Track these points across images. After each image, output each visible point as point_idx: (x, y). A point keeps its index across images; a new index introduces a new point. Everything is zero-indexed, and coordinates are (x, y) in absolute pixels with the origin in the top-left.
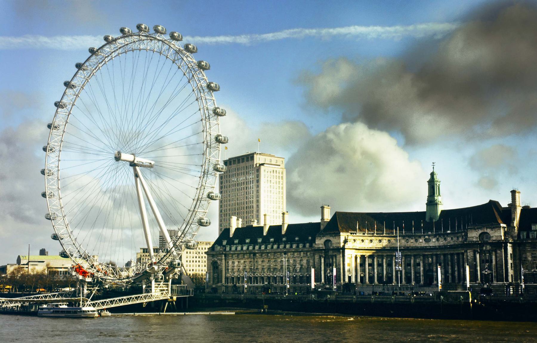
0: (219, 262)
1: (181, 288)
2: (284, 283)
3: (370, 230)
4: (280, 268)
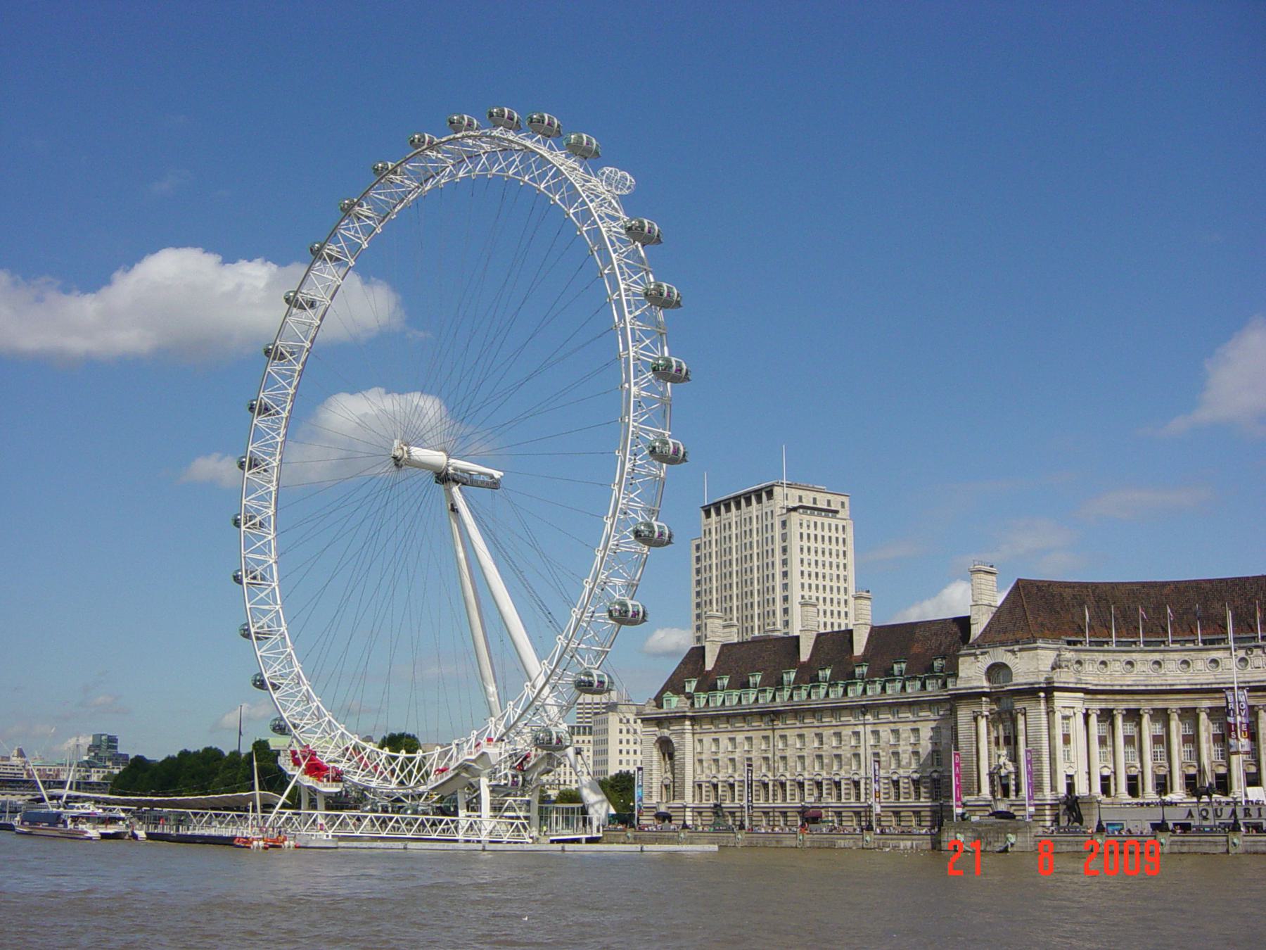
0: (674, 739)
1: (567, 813)
2: (862, 800)
3: (1125, 633)
4: (849, 755)
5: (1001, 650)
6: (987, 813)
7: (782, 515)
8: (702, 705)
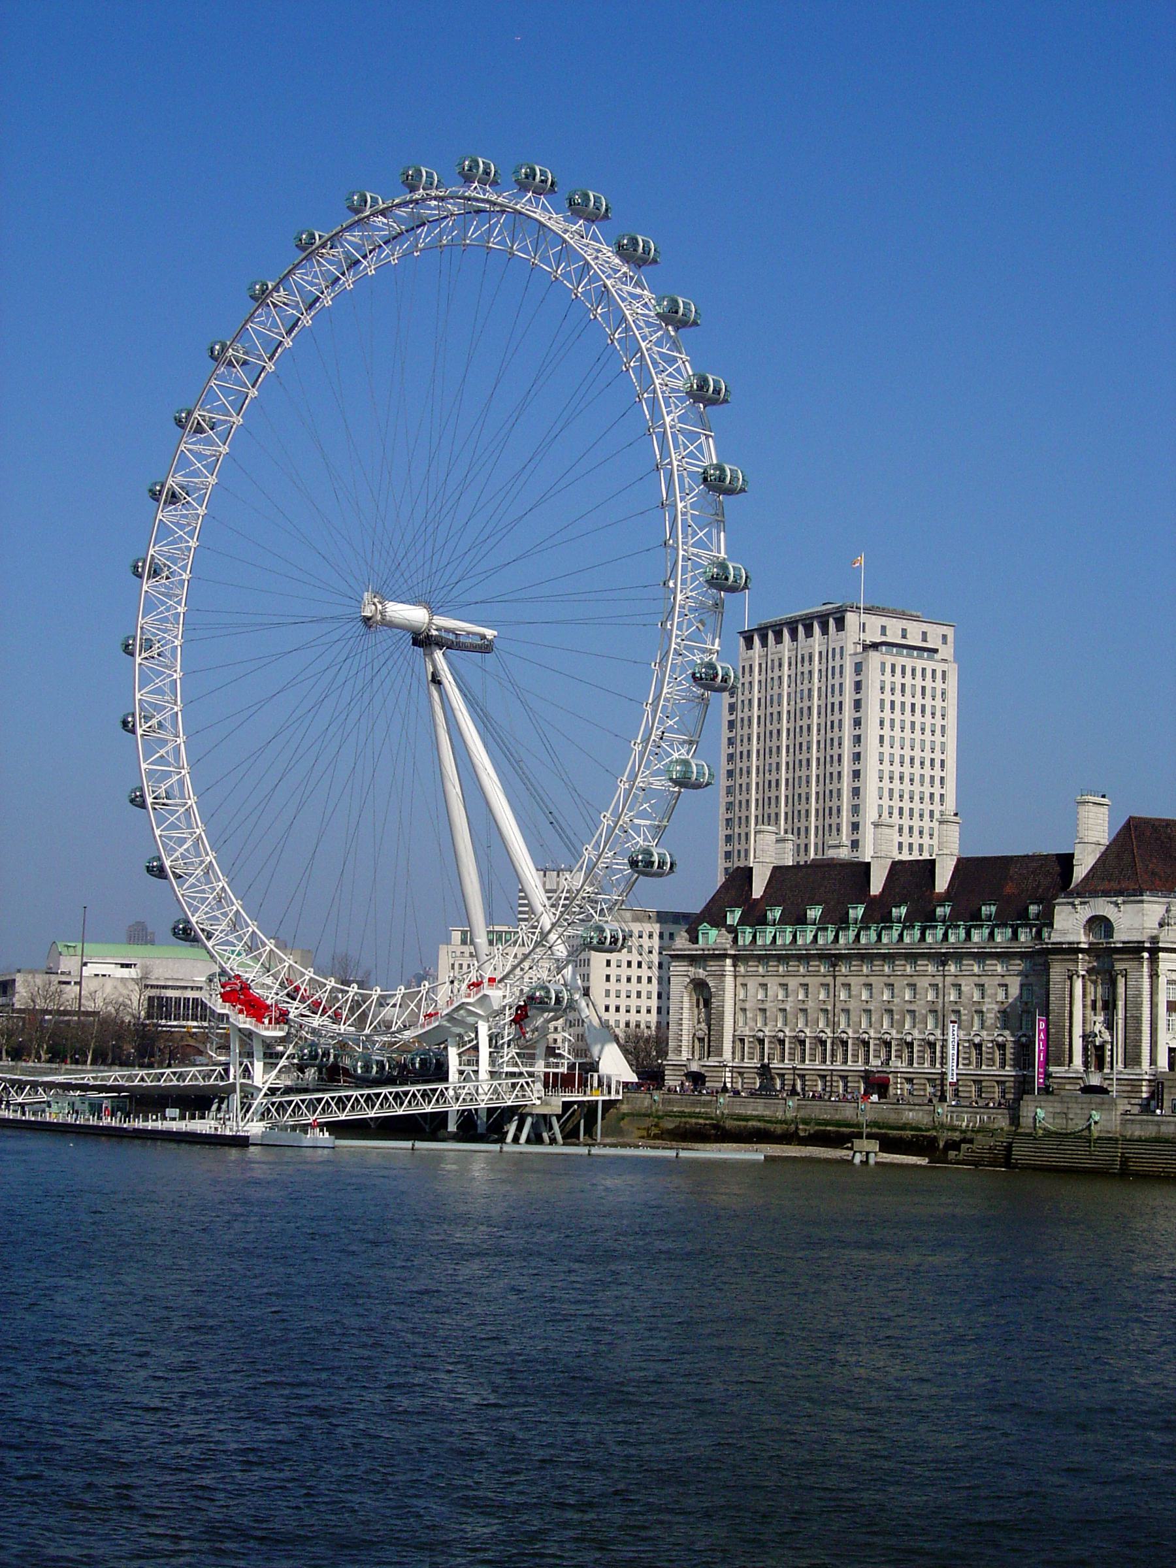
4: (924, 1012)
5: (1101, 900)
6: (1078, 1087)
7: (856, 654)
8: (747, 943)
